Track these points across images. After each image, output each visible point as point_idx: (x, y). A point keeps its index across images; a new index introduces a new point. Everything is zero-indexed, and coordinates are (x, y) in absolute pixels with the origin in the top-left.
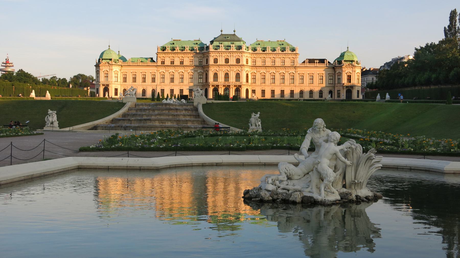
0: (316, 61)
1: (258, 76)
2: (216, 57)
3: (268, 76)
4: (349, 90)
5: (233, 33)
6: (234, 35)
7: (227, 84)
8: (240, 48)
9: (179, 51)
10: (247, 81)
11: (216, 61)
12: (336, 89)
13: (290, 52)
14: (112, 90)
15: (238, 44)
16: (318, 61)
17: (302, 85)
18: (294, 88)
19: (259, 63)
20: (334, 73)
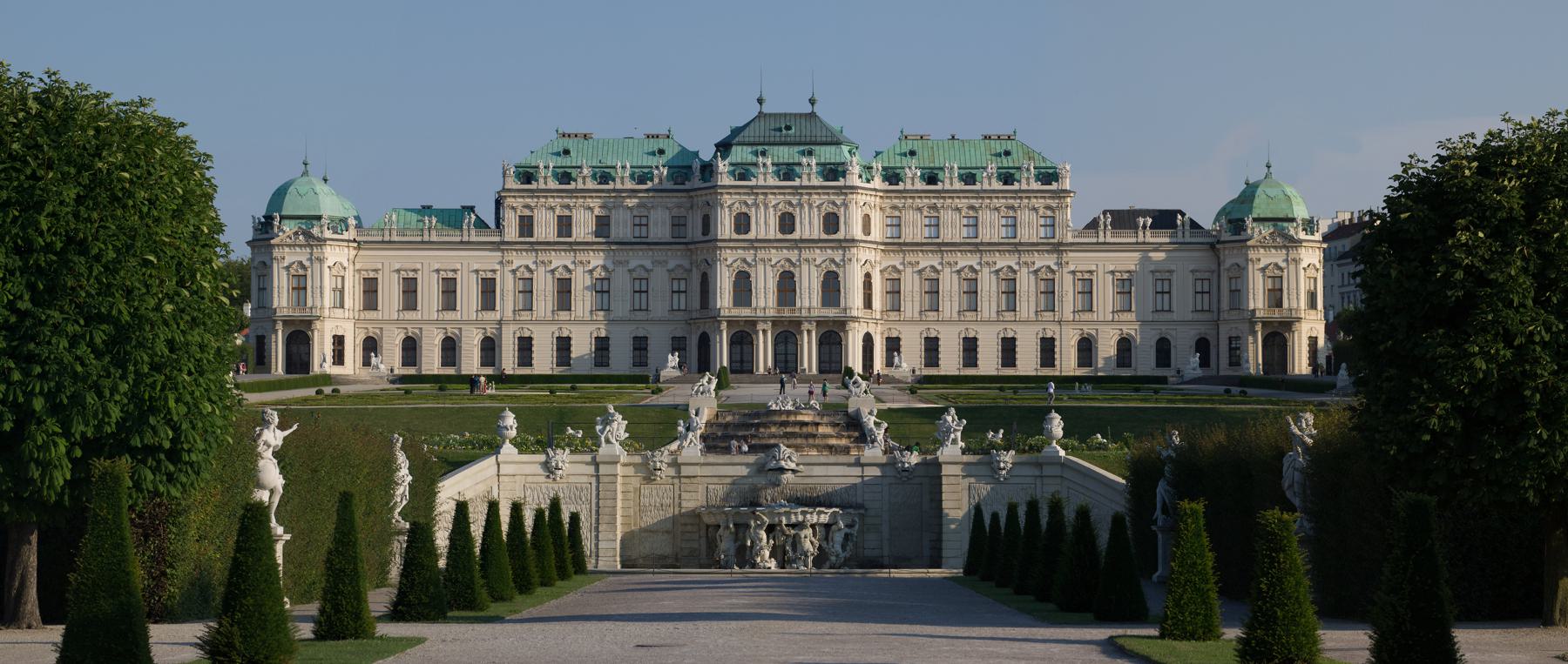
0: (1141, 221)
1: (911, 286)
2: (744, 209)
3: (950, 284)
4: (1277, 337)
5: (808, 109)
6: (812, 115)
7: (786, 313)
8: (834, 172)
9: (591, 185)
10: (868, 304)
11: (742, 223)
12: (1225, 332)
13: (1036, 186)
14: (322, 343)
15: (827, 154)
16: (1150, 221)
17: (1087, 316)
18: (1056, 328)
19: (916, 228)
20: (1214, 267)
